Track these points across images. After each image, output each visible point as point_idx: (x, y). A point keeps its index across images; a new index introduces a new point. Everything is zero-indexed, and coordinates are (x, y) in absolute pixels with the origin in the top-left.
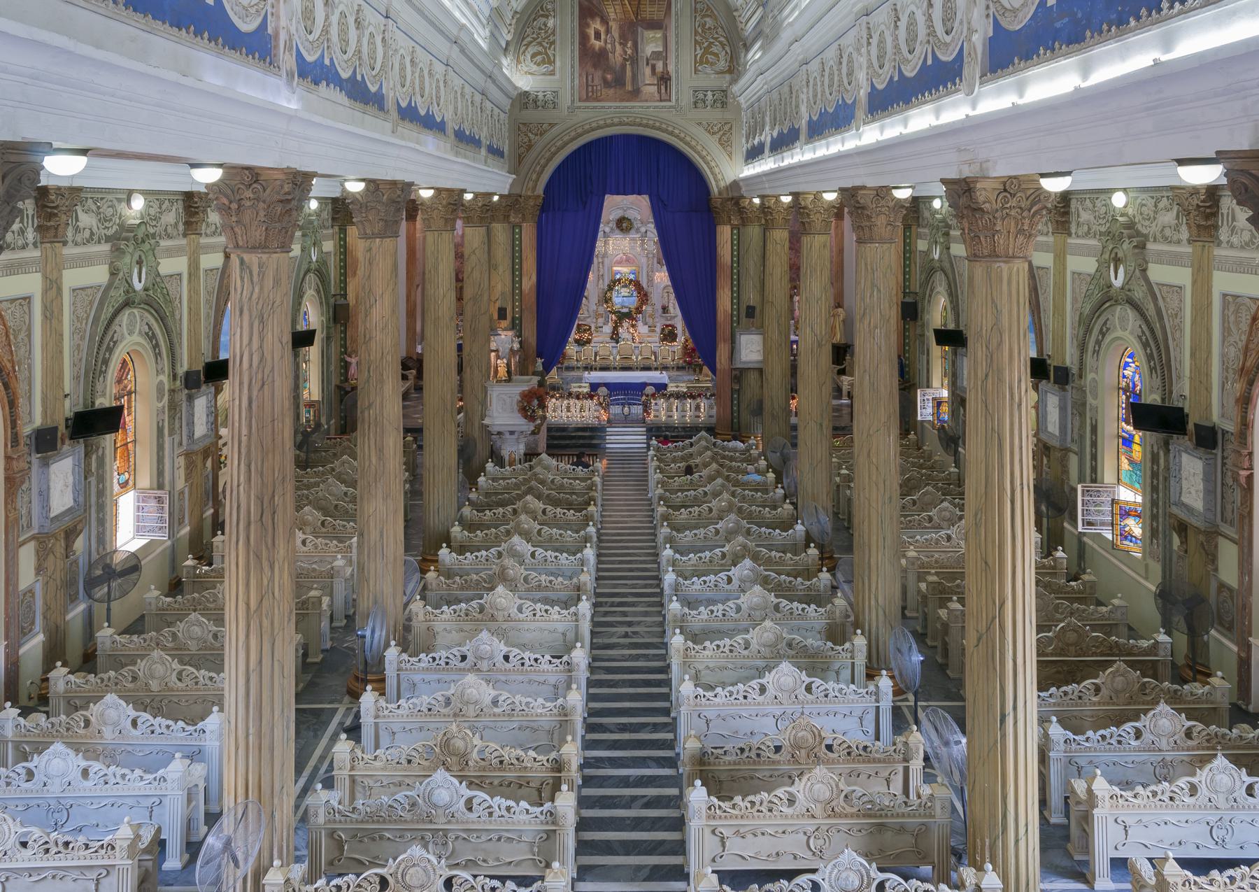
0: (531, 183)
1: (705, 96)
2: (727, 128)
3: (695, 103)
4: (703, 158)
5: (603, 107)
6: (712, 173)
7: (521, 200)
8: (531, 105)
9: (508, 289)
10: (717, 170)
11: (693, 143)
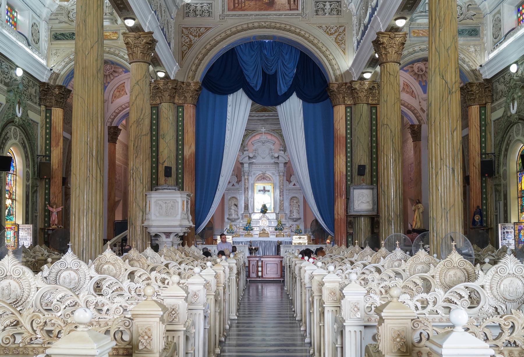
0: (191, 73)
1: (324, 5)
2: (341, 30)
3: (317, 11)
4: (323, 53)
5: (247, 15)
6: (330, 64)
7: (184, 86)
8: (192, 14)
9: (173, 154)
10: (334, 62)
11: (316, 41)
